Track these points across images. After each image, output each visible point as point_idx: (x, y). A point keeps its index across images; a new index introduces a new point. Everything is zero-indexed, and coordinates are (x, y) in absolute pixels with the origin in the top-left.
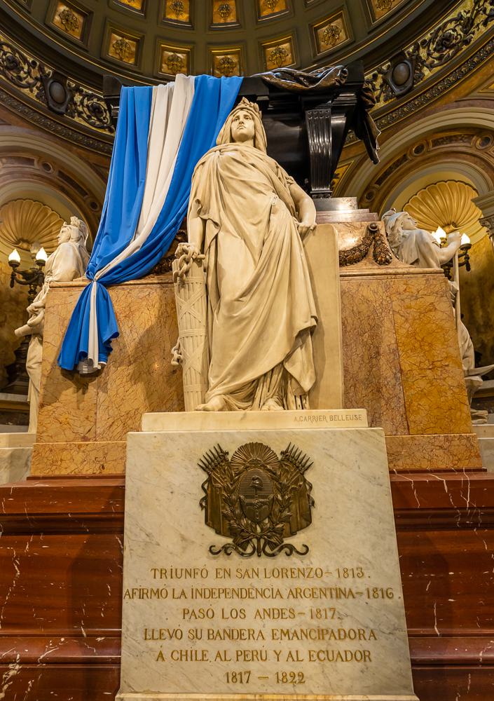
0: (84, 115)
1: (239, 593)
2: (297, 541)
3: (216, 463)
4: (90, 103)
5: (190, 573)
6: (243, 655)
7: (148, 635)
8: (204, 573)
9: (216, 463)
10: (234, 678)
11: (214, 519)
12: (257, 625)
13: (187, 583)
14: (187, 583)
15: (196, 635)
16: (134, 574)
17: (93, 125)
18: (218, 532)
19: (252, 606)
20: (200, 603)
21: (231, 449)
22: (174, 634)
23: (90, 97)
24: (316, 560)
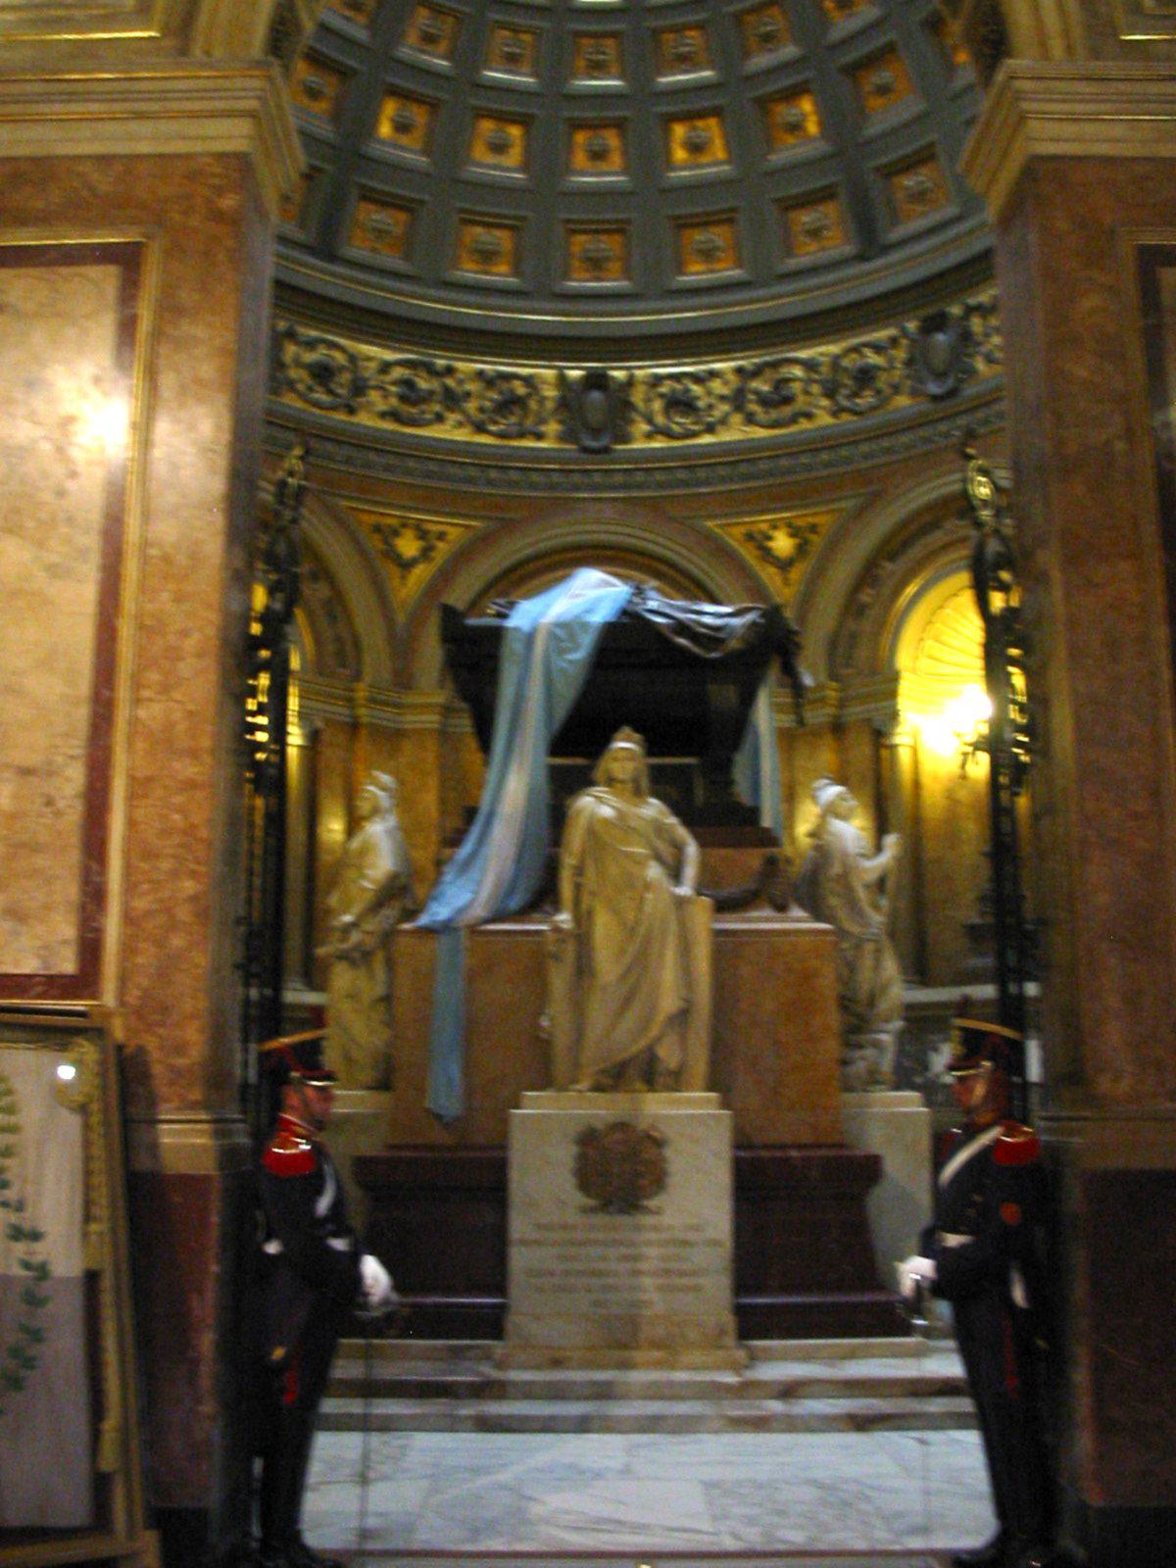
0: (300, 387)
1: (604, 1244)
2: (652, 1203)
3: (588, 1139)
4: (309, 357)
5: (565, 1227)
6: (606, 1288)
7: (530, 1273)
8: (574, 1227)
9: (588, 1139)
10: (597, 1304)
11: (585, 1183)
12: (614, 1266)
13: (559, 1235)
14: (559, 1235)
15: (567, 1273)
16: (519, 1226)
17: (316, 404)
18: (589, 1195)
19: (611, 1252)
20: (574, 1250)
21: (599, 1125)
22: (552, 1274)
23: (311, 344)
24: (666, 1219)
